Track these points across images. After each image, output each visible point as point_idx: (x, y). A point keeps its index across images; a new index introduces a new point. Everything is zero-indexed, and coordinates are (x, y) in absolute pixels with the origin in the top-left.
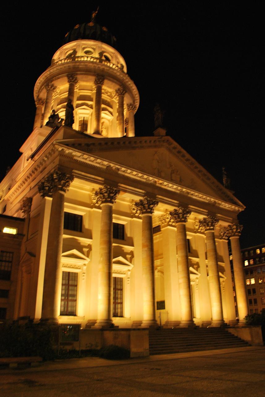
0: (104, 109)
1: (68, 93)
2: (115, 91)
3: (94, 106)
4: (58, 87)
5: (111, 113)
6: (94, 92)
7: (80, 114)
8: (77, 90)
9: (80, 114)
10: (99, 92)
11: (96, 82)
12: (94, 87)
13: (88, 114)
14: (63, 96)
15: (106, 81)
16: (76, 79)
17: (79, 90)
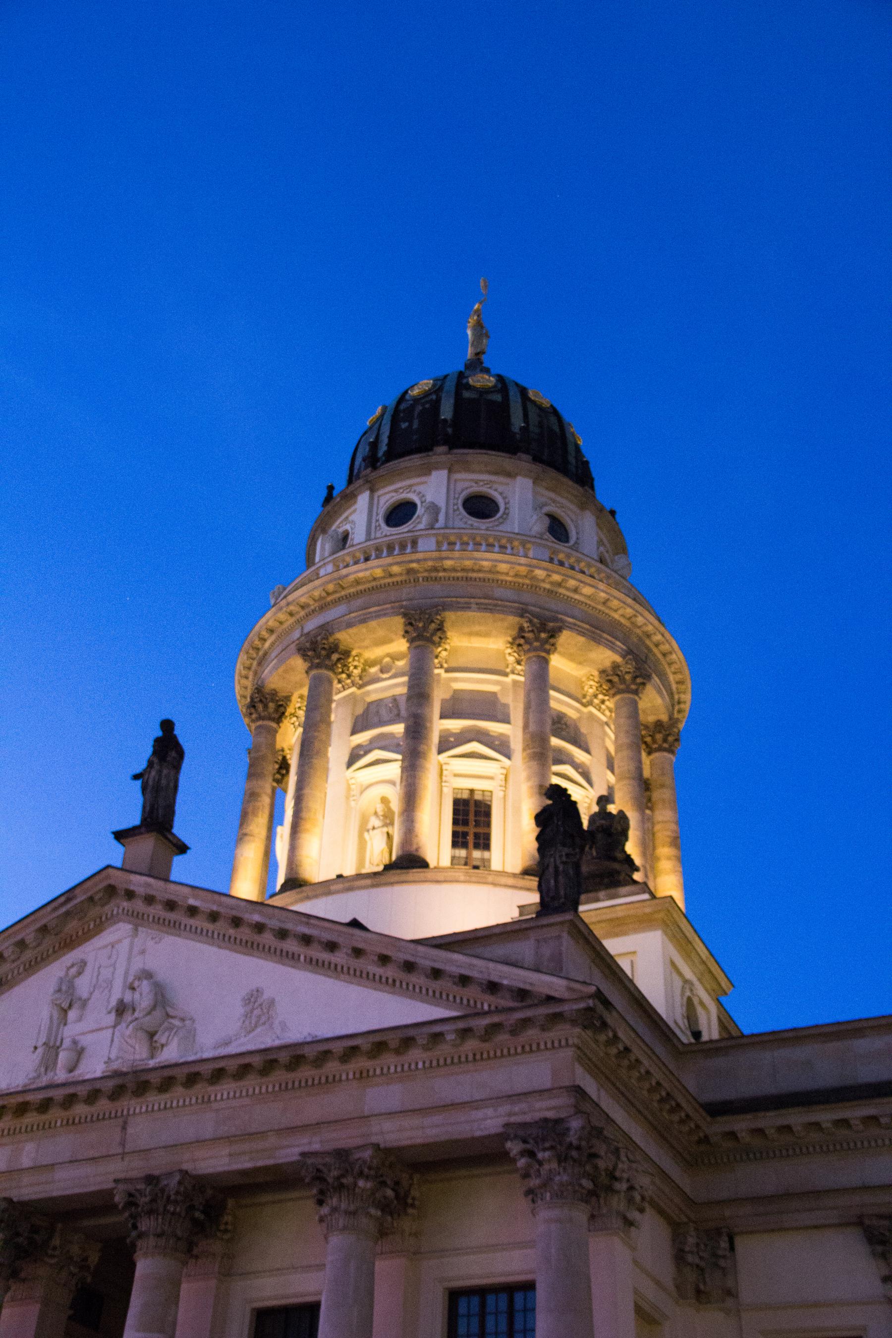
0: (561, 758)
1: (405, 679)
2: (596, 673)
3: (517, 743)
4: (354, 653)
5: (586, 775)
6: (515, 682)
7: (456, 775)
8: (441, 671)
9: (456, 775)
10: (540, 683)
11: (520, 640)
12: (511, 659)
13: (491, 778)
14: (376, 691)
15: (566, 638)
16: (441, 628)
17: (447, 671)
